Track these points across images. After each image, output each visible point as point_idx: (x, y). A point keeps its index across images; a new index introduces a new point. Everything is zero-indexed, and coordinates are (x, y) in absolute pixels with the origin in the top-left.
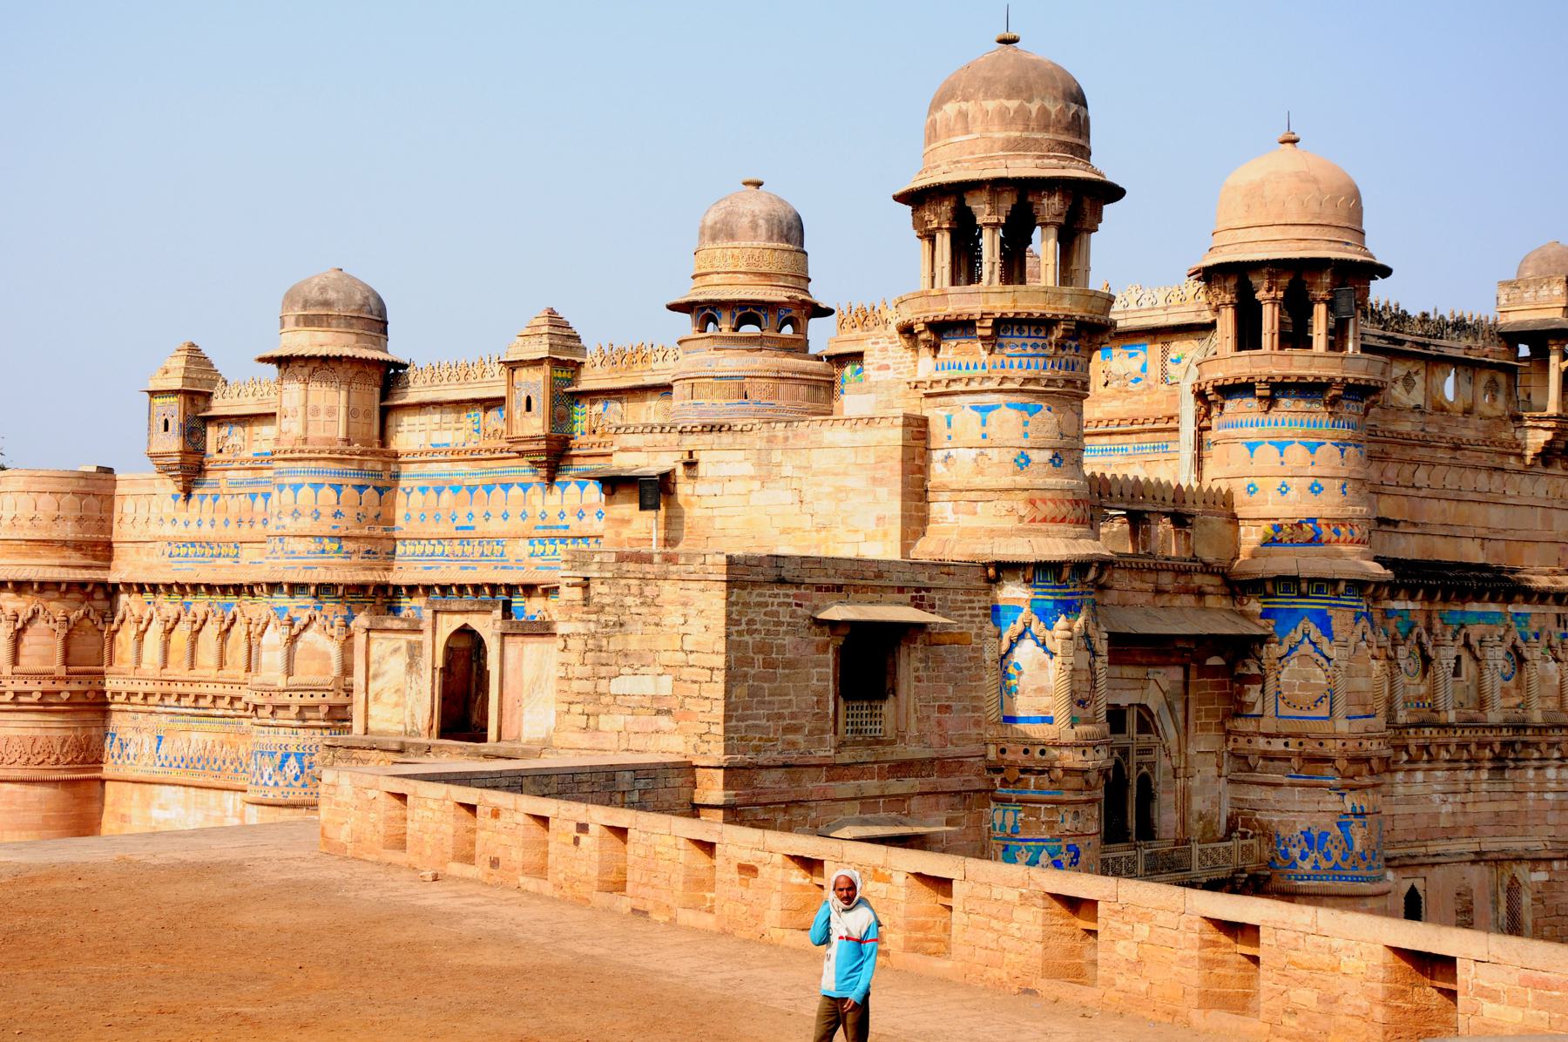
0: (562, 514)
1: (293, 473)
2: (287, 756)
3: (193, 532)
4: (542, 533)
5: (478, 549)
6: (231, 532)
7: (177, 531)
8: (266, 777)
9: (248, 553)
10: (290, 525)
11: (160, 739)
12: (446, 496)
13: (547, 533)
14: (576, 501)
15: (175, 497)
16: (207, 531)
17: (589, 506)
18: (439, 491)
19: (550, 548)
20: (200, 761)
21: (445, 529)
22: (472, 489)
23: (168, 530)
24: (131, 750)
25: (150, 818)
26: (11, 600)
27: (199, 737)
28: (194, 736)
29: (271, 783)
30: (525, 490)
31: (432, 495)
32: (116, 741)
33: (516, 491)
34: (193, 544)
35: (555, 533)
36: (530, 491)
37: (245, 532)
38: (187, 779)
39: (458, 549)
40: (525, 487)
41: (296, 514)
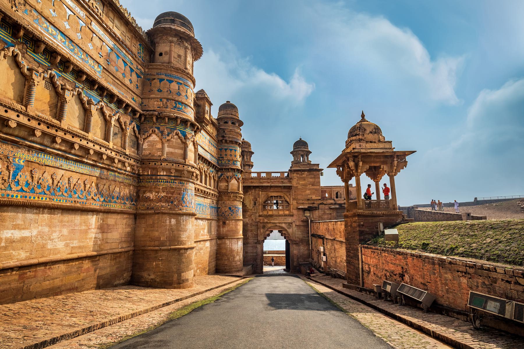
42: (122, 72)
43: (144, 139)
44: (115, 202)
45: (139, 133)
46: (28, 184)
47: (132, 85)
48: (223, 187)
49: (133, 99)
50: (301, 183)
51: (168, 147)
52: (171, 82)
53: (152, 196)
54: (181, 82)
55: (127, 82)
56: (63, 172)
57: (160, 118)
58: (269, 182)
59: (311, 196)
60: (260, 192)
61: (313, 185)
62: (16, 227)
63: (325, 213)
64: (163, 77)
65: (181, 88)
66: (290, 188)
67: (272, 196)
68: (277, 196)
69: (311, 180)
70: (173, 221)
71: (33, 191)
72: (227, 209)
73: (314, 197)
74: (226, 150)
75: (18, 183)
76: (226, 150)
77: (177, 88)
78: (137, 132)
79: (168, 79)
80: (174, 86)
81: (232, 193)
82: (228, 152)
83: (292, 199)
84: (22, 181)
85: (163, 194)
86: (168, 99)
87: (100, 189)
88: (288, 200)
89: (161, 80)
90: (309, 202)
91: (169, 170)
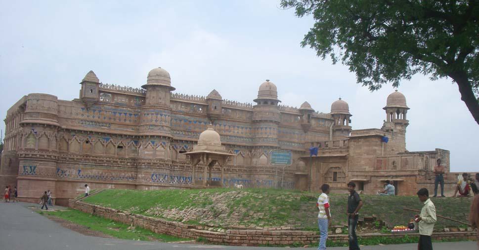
1: (165, 112)
2: (166, 175)
3: (91, 118)
5: (193, 134)
6: (106, 120)
7: (85, 117)
8: (161, 180)
9: (113, 127)
10: (164, 124)
11: (80, 171)
12: (182, 122)
14: (219, 128)
15: (83, 109)
16: (96, 119)
17: (222, 129)
18: (181, 121)
20: (100, 177)
21: (182, 129)
22: (190, 121)
23: (80, 117)
24: (67, 173)
25: (76, 191)
26: (49, 130)
27: (95, 172)
28: (94, 170)
31: (178, 121)
33: (203, 123)
34: (92, 122)
37: (112, 121)
38: (92, 181)
39: (187, 133)
40: (205, 123)
41: (165, 121)
42: (124, 119)
43: (139, 148)
48: (255, 163)
49: (132, 129)
50: (357, 152)
51: (147, 151)
52: (148, 114)
53: (140, 176)
55: (127, 122)
57: (142, 136)
58: (330, 152)
59: (364, 167)
60: (322, 163)
61: (368, 154)
62: (81, 188)
63: (376, 187)
64: (145, 112)
66: (344, 158)
67: (332, 168)
68: (336, 168)
69: (366, 148)
70: (147, 189)
72: (256, 181)
73: (367, 168)
74: (258, 128)
78: (135, 145)
80: (150, 117)
81: (259, 167)
83: (347, 171)
86: (146, 125)
88: (344, 171)
89: (145, 114)
90: (363, 174)
91: (144, 163)
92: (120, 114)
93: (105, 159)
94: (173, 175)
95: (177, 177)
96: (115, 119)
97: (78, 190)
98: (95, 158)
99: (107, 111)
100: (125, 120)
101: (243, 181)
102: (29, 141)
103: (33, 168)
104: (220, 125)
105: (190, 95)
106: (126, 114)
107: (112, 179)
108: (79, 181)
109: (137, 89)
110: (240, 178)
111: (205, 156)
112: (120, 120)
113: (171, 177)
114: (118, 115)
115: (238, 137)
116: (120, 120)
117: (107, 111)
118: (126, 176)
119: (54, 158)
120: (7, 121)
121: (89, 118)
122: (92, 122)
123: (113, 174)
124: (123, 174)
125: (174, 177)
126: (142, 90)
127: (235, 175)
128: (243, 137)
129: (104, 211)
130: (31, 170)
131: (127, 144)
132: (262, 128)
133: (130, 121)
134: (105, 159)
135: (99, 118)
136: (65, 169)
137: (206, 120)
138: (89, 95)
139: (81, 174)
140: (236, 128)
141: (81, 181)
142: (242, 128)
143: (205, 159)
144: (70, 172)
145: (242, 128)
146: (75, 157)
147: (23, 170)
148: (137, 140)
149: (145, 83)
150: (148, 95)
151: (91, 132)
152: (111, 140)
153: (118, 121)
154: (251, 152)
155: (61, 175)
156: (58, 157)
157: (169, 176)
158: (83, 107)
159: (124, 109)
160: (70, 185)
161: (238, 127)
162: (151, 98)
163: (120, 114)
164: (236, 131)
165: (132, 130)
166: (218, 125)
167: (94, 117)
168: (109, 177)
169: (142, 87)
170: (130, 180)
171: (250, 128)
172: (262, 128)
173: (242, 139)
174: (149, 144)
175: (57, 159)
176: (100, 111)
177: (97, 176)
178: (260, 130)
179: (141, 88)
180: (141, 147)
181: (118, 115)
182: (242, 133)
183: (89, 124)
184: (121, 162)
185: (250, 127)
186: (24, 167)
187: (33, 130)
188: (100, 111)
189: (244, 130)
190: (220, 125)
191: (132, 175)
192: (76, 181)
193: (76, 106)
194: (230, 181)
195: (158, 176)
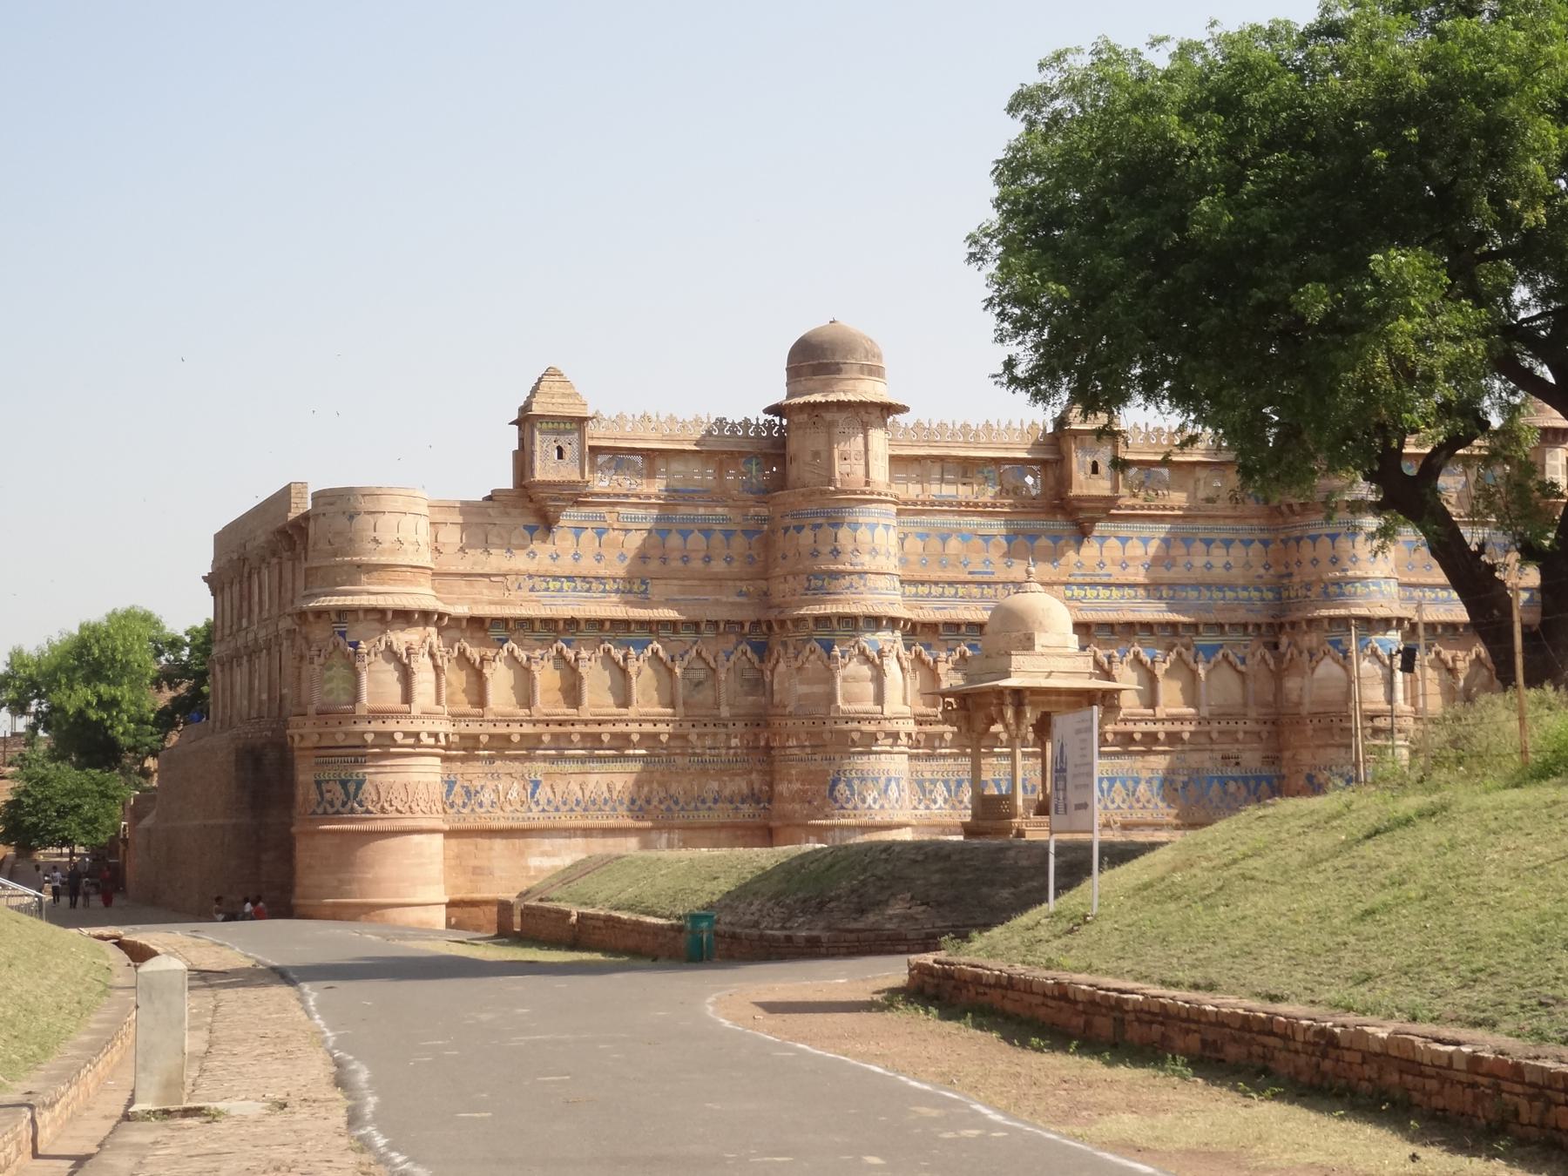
0: (1102, 564)
2: (889, 780)
3: (566, 565)
4: (1080, 579)
8: (870, 800)
11: (536, 784)
12: (954, 544)
13: (1088, 580)
14: (1118, 554)
16: (588, 566)
17: (1133, 558)
18: (944, 539)
19: (1091, 593)
24: (487, 797)
25: (527, 868)
28: (593, 779)
29: (877, 807)
30: (1055, 543)
32: (457, 788)
34: (570, 578)
35: (1097, 580)
36: (1062, 542)
38: (590, 823)
40: (1056, 538)
42: (702, 554)
43: (772, 671)
44: (710, 809)
45: (762, 661)
46: (549, 802)
47: (735, 564)
49: (740, 594)
51: (802, 682)
52: (799, 529)
54: (819, 521)
56: (597, 777)
62: (544, 854)
64: (788, 521)
65: (821, 536)
71: (557, 809)
74: (1298, 540)
75: (537, 803)
76: (1298, 540)
77: (811, 540)
78: (755, 659)
79: (796, 523)
80: (807, 537)
82: (1307, 550)
84: (543, 801)
85: (797, 786)
87: (672, 791)
89: (786, 530)
92: (685, 534)
93: (634, 727)
94: (928, 775)
95: (946, 783)
96: (664, 560)
97: (535, 862)
98: (594, 729)
99: (627, 531)
100: (707, 559)
101: (1246, 780)
102: (331, 679)
103: (352, 788)
104: (1124, 541)
105: (976, 422)
106: (707, 533)
107: (669, 809)
108: (535, 824)
109: (746, 423)
110: (1235, 772)
111: (1008, 700)
112: (685, 559)
113: (921, 784)
114: (674, 540)
115: (1209, 586)
116: (685, 559)
117: (627, 531)
118: (727, 792)
119: (432, 741)
120: (216, 582)
121: (558, 562)
122: (570, 578)
123: (675, 788)
124: (715, 785)
125: (933, 782)
126: (770, 426)
127: (1207, 755)
128: (1232, 587)
129: (600, 924)
130: (347, 794)
131: (722, 657)
132: (1314, 539)
133: (729, 560)
134: (634, 727)
135: (599, 558)
136: (477, 783)
137: (1059, 524)
138: (546, 469)
139: (544, 793)
140: (1199, 547)
141: (543, 823)
142: (1228, 543)
143: (1009, 713)
144: (496, 791)
145: (1228, 543)
146: (515, 729)
147: (314, 795)
148: (762, 639)
149: (778, 393)
150: (793, 446)
151: (572, 623)
152: (656, 645)
153: (679, 564)
154: (1276, 646)
155: (464, 805)
156: (447, 736)
157: (902, 783)
158: (532, 521)
159: (701, 511)
160: (499, 844)
161: (1208, 543)
162: (808, 458)
163: (685, 534)
164: (1199, 561)
165: (739, 599)
166: (1113, 542)
167: (576, 557)
168: (655, 802)
169: (768, 411)
170: (746, 809)
171: (1265, 543)
172: (1314, 539)
173: (1229, 594)
174: (812, 652)
175: (443, 742)
176: (600, 532)
177: (606, 802)
178: (1306, 547)
179: (764, 417)
180: (782, 667)
181: (674, 540)
182: (1227, 566)
183: (561, 590)
184: (699, 736)
185: (1265, 536)
186: (318, 783)
187: (343, 634)
188: (600, 532)
189: (1237, 551)
190: (1124, 541)
191: (751, 784)
192: (525, 825)
193: (506, 521)
194: (1185, 785)
195: (856, 784)
